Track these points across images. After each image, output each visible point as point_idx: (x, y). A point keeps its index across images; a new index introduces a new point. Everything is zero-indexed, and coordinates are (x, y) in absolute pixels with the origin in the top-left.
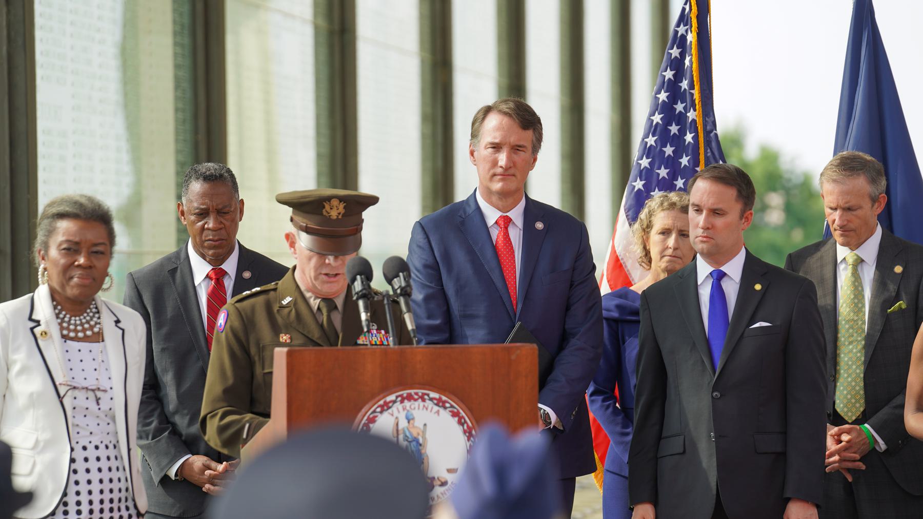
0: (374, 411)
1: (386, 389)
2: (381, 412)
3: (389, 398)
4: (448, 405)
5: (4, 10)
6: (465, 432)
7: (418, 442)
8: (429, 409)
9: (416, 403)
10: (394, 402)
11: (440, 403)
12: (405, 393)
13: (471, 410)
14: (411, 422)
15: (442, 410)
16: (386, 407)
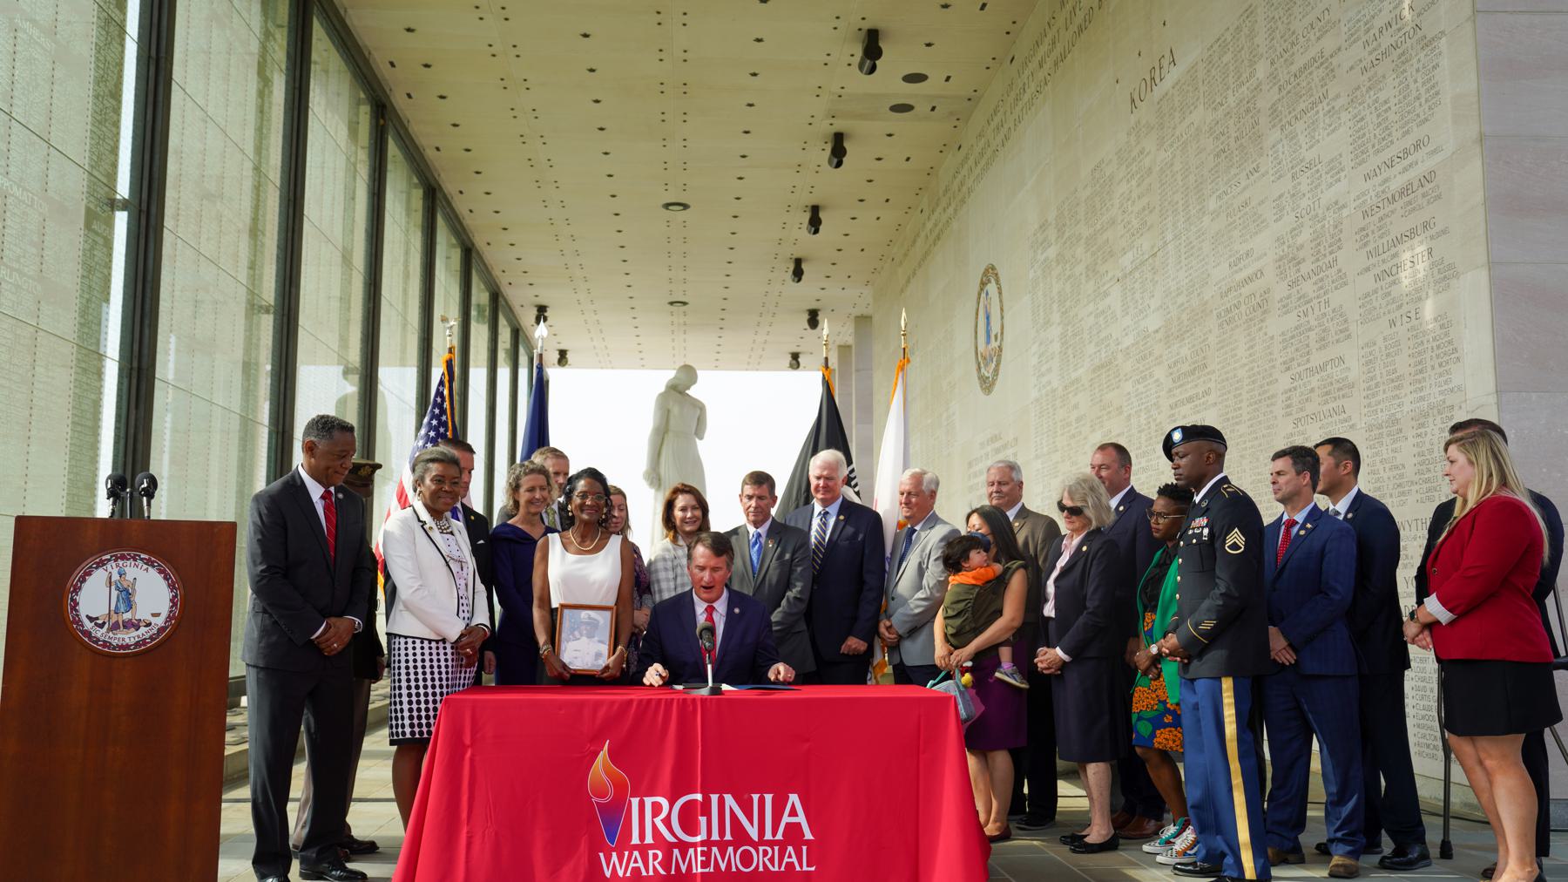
0: (91, 567)
1: (104, 551)
2: (96, 568)
3: (104, 558)
4: (156, 564)
5: (134, 412)
6: (169, 585)
7: (128, 591)
8: (139, 567)
9: (129, 562)
10: (109, 560)
11: (149, 563)
12: (119, 554)
13: (177, 570)
14: (123, 576)
15: (150, 568)
16: (101, 564)
